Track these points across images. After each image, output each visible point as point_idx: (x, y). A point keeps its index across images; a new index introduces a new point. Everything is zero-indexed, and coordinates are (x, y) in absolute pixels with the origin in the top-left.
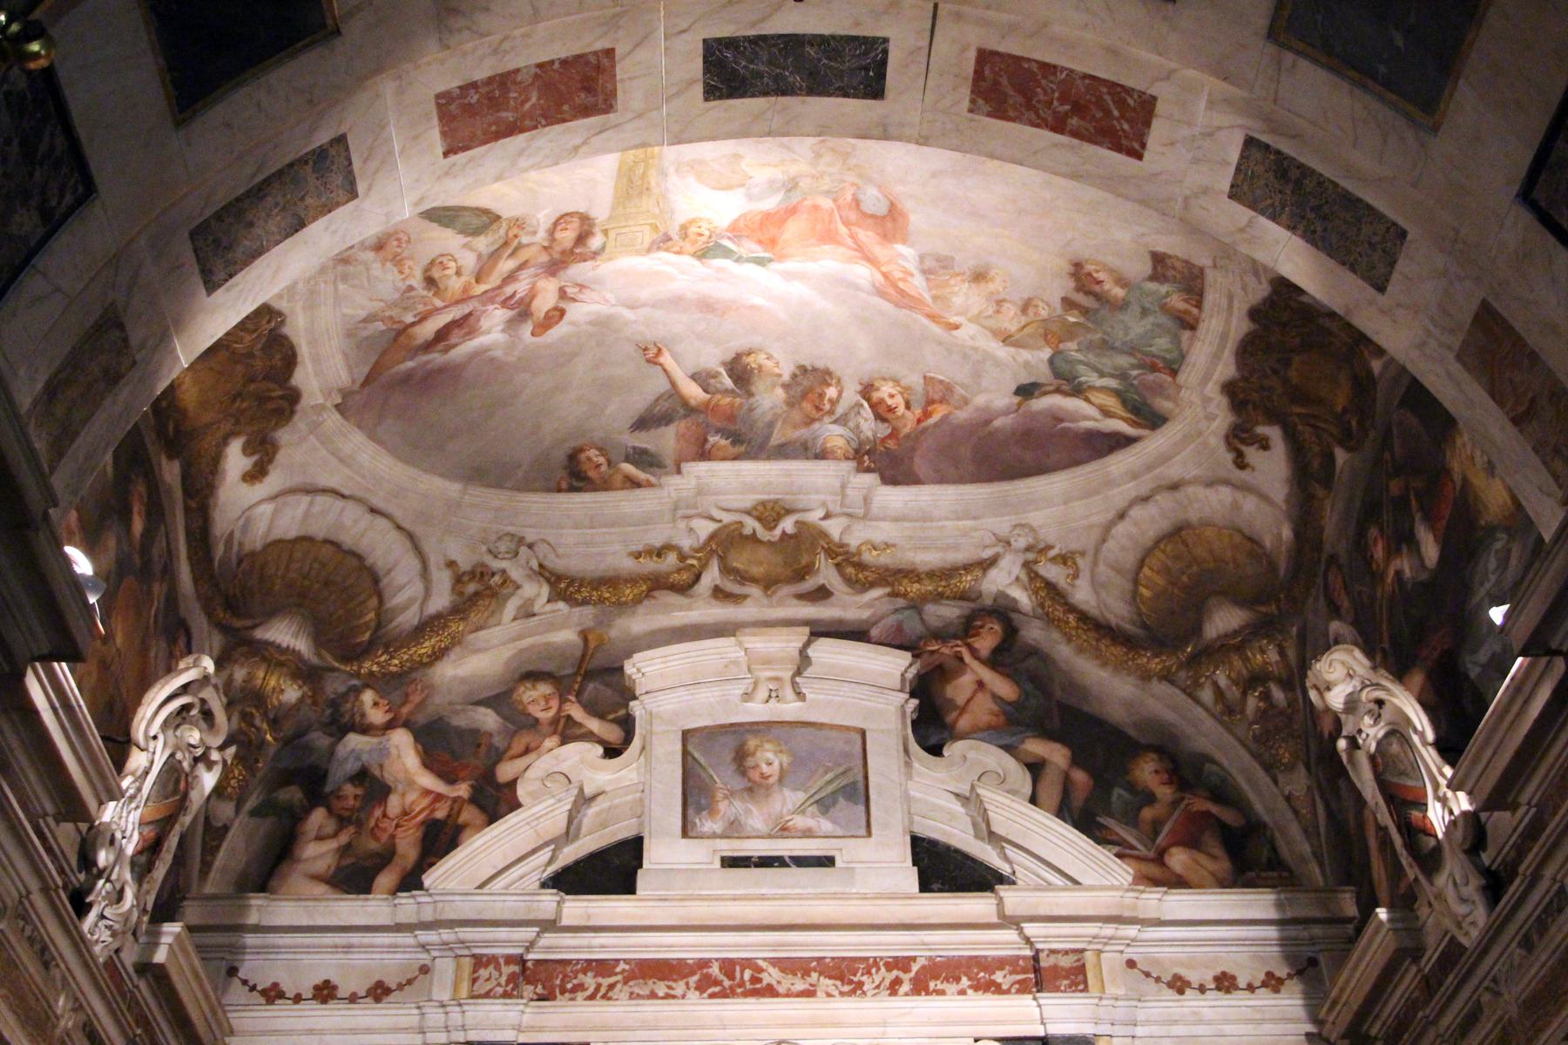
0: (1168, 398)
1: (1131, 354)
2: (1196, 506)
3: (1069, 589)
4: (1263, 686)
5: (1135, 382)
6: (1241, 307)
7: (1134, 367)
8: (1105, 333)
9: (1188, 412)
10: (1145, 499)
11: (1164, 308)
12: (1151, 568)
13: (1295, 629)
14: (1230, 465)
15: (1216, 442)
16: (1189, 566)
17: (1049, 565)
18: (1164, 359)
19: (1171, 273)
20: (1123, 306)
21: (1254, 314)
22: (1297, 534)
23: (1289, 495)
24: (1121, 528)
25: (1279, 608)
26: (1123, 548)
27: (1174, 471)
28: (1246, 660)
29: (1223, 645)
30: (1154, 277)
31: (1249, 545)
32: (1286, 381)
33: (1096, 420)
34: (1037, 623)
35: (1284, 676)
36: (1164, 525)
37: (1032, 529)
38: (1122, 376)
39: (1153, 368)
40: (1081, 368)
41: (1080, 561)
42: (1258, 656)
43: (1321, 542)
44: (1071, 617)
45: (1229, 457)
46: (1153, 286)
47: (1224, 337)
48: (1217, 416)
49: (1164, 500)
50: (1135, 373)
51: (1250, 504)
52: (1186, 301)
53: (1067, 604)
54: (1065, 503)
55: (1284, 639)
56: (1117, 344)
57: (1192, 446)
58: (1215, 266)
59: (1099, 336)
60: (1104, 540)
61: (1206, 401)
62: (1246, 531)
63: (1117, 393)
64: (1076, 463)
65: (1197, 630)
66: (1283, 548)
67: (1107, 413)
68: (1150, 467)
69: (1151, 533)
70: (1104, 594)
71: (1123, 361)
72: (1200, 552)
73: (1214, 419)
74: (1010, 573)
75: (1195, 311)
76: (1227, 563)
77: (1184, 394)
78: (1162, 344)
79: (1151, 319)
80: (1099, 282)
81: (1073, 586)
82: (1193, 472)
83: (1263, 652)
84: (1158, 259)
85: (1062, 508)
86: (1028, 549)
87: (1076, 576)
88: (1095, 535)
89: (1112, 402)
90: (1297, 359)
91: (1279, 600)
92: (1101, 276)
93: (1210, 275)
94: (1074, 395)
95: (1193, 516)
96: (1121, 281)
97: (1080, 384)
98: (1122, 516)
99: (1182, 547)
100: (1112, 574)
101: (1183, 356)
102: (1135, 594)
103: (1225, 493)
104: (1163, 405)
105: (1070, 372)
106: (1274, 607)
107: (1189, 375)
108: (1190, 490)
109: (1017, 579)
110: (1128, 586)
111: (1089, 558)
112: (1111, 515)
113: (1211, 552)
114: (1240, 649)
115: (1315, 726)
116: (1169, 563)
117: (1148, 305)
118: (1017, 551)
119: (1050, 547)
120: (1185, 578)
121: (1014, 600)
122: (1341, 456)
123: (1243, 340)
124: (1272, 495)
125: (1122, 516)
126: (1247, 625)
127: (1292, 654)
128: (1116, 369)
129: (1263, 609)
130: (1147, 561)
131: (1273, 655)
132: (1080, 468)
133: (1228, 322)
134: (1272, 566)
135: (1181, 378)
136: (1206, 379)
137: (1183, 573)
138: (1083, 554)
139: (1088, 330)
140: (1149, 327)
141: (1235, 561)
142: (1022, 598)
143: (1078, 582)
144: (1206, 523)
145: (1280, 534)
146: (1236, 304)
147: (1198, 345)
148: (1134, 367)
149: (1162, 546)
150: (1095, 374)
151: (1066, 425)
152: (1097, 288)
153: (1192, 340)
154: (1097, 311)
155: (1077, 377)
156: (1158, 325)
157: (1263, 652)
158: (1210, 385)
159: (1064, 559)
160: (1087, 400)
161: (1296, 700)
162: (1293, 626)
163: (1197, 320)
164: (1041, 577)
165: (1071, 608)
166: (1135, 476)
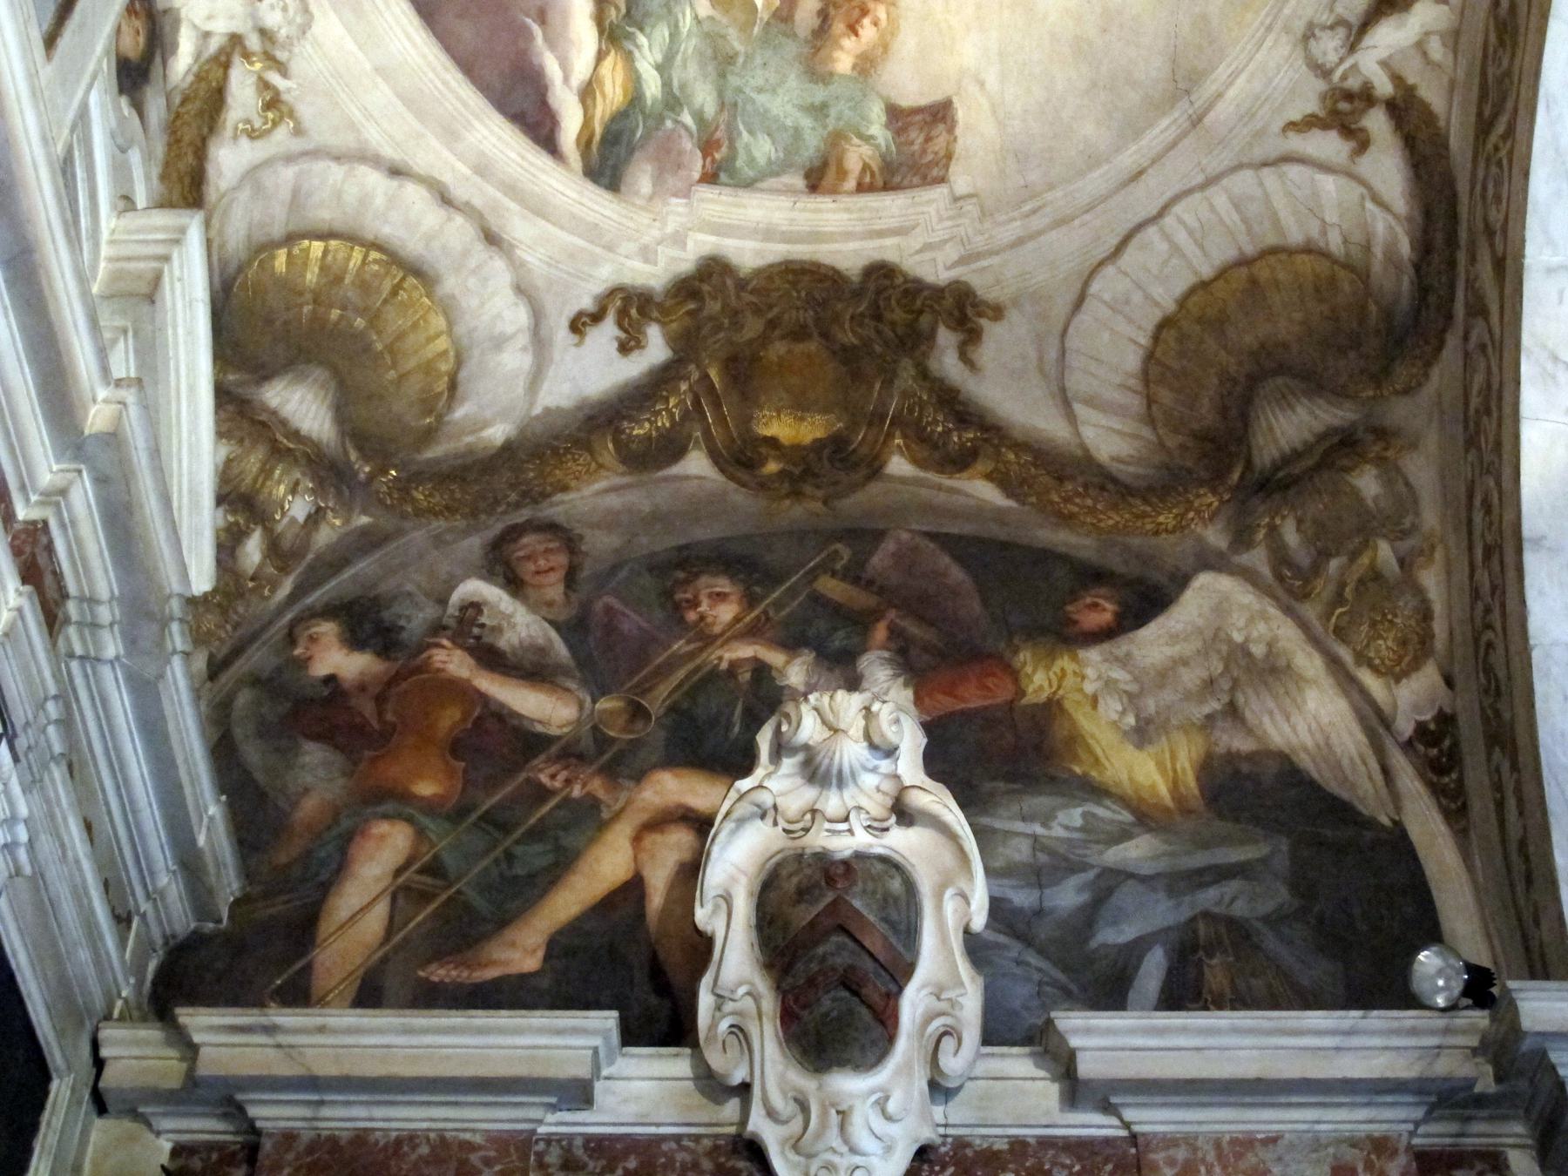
0: (658, 180)
1: (722, 106)
2: (472, 282)
3: (228, 132)
4: (248, 521)
5: (669, 124)
6: (887, 250)
7: (699, 117)
8: (749, 58)
9: (644, 219)
10: (445, 199)
11: (836, 140)
12: (326, 252)
13: (364, 520)
14: (570, 311)
15: (604, 275)
16: (362, 312)
17: (251, 80)
18: (732, 157)
19: (917, 137)
20: (816, 72)
21: (880, 273)
22: (508, 449)
23: (559, 410)
24: (374, 180)
25: (371, 478)
26: (338, 195)
27: (520, 228)
28: (265, 471)
29: (263, 424)
30: (897, 116)
31: (442, 385)
32: (764, 340)
33: (566, 79)
34: (162, 101)
35: (286, 543)
36: (412, 246)
37: (304, 29)
38: (673, 101)
39: (707, 146)
40: (662, 32)
41: (282, 134)
42: (282, 488)
43: (545, 496)
44: (190, 159)
45: (587, 303)
46: (877, 113)
47: (815, 237)
48: (655, 264)
49: (459, 232)
50: (687, 118)
51: (515, 360)
52: (866, 167)
53: (204, 140)
54: (378, 70)
55: (332, 510)
56: (734, 81)
57: (581, 243)
58: (956, 199)
59: (738, 46)
60: (338, 158)
61: (679, 239)
62: (463, 375)
63: (635, 99)
64: (468, 66)
65: (265, 374)
66: (469, 439)
67: (587, 94)
68: (512, 190)
69: (389, 230)
70: (244, 195)
71: (704, 97)
72: (395, 321)
73: (646, 261)
74: (210, 17)
75: (851, 184)
76: (394, 365)
77: (677, 204)
78: (763, 149)
79: (806, 122)
80: (853, 29)
81: (235, 138)
82: (533, 258)
83: (293, 490)
84: (940, 114)
85: (368, 66)
86: (265, 34)
87: (253, 135)
88: (342, 140)
89: (613, 94)
90: (812, 346)
91: (385, 472)
92: (868, 31)
93: (936, 196)
94: (601, 33)
95: (450, 284)
96: (866, 65)
97: (630, 37)
98: (396, 171)
99: (387, 286)
100: (285, 194)
101: (749, 185)
102: (269, 246)
103: (516, 317)
104: (642, 177)
105: (647, 15)
106: (367, 469)
107: (715, 203)
108: (498, 264)
109: (207, 35)
110: (277, 231)
111: (297, 145)
112: (388, 152)
113: (401, 336)
114: (277, 452)
115: (291, 639)
116: (347, 281)
117: (833, 112)
118: (254, 16)
119: (282, 68)
120: (335, 314)
121: (174, 46)
122: (696, 464)
123: (818, 265)
124: (546, 386)
125: (396, 171)
126: (316, 445)
127: (325, 536)
128: (682, 87)
129: (353, 456)
130: (333, 243)
131: (299, 508)
132: (460, 76)
133: (848, 236)
134: (428, 436)
135: (706, 192)
136: (719, 230)
137: (344, 308)
138: (298, 131)
139: (746, 27)
140: (789, 122)
141: (402, 377)
142: (183, 61)
143: (244, 142)
144: (448, 309)
145: (486, 424)
146: (889, 242)
147: (784, 202)
148: (699, 117)
149: (374, 255)
150: (659, 58)
151: (537, 30)
152: (839, 27)
153: (789, 191)
154: (793, 36)
155: (641, 29)
156: (797, 133)
157: (293, 490)
158: (713, 239)
159: (273, 102)
160: (600, 57)
161: (275, 586)
162: (364, 512)
163: (834, 191)
164: (225, 77)
165: (201, 153)
166: (482, 169)
